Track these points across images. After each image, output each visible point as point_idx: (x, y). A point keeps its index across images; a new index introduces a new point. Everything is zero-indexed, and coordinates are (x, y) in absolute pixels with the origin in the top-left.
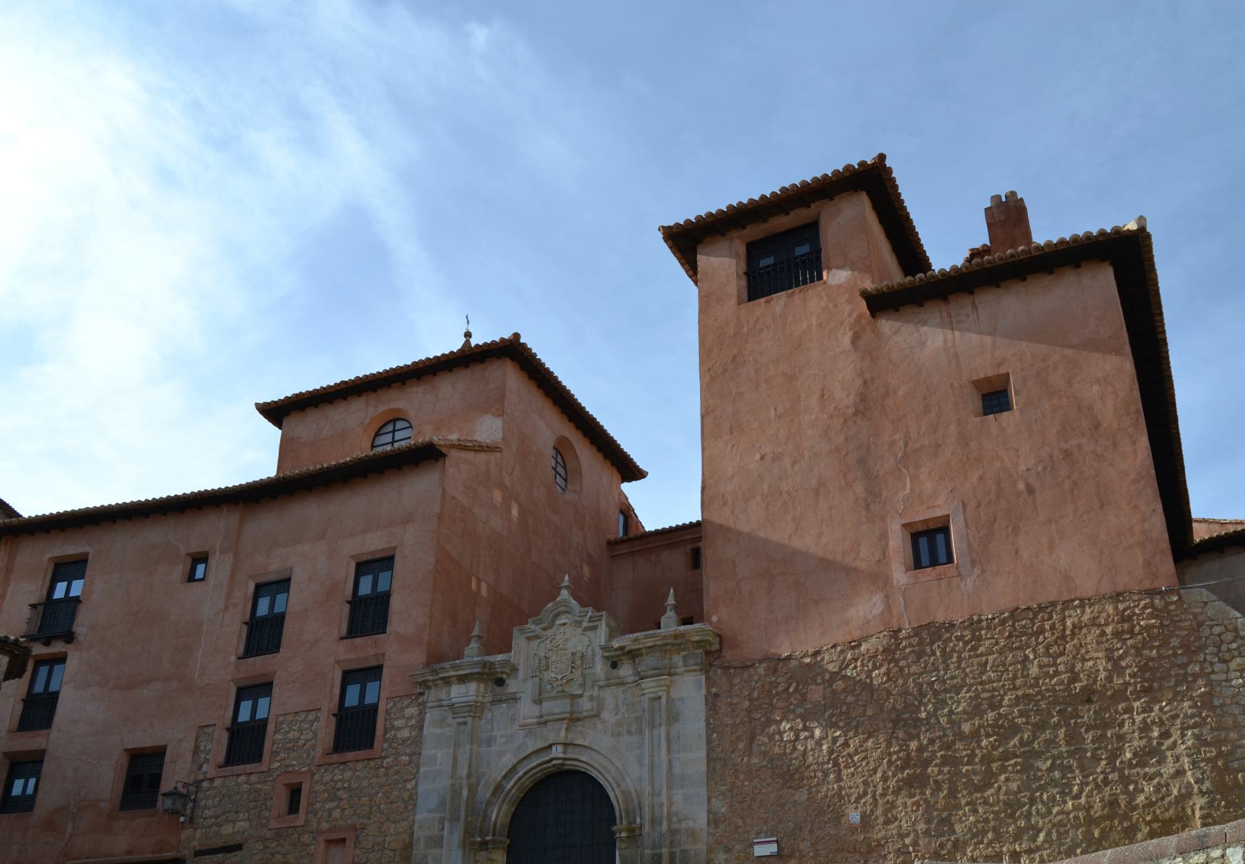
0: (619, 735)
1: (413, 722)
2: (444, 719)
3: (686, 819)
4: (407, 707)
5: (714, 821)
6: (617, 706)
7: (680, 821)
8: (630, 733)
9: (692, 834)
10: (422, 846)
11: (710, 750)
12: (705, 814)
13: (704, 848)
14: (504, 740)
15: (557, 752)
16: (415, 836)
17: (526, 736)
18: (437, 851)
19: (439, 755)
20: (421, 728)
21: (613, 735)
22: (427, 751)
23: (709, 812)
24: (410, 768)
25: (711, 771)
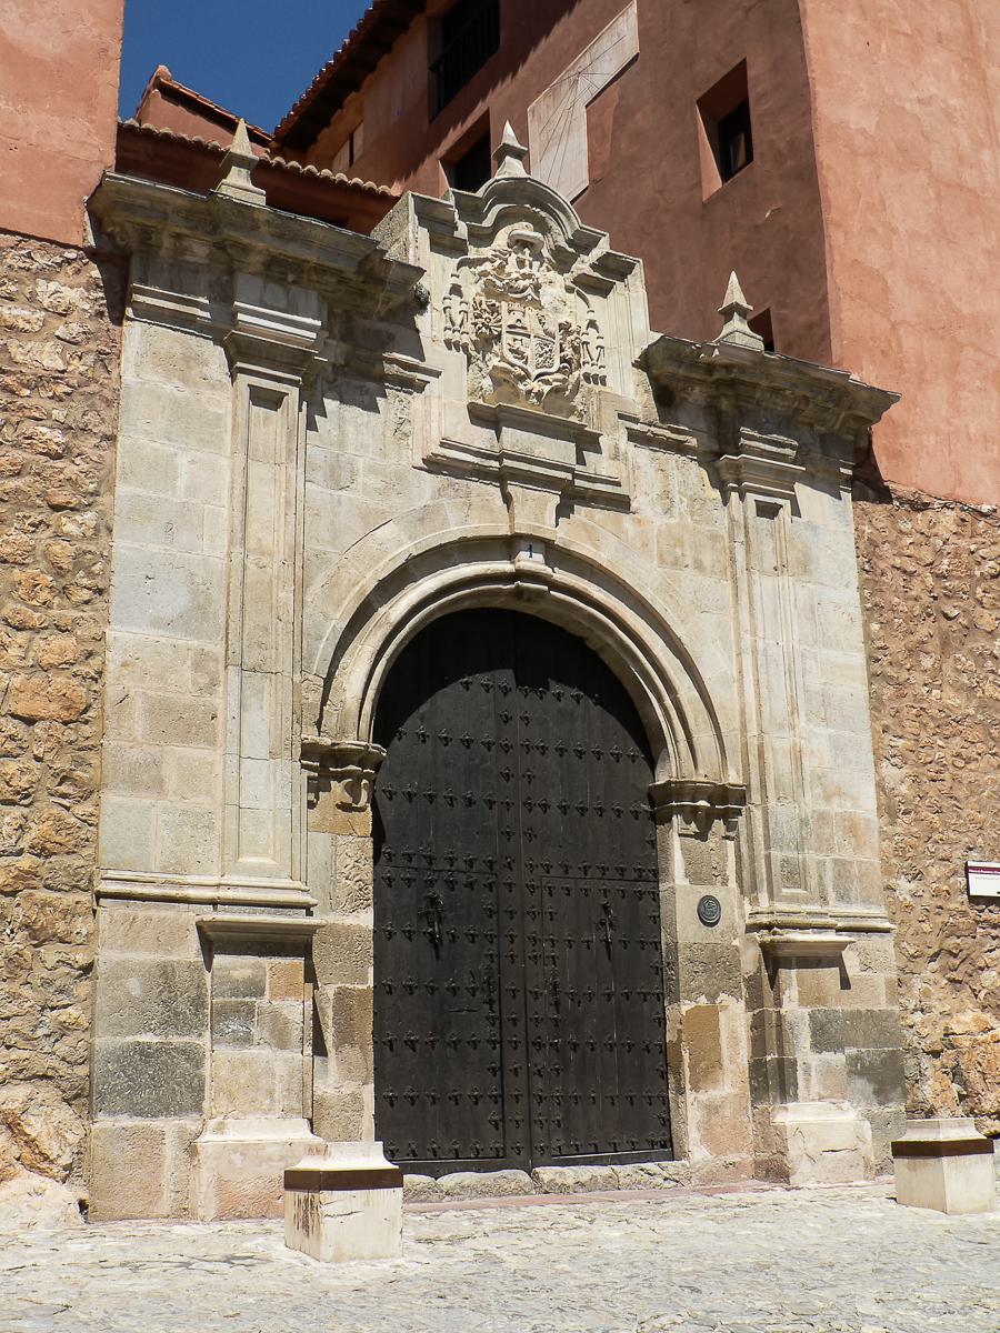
0: (675, 563)
1: (74, 328)
2: (191, 359)
3: (840, 793)
4: (47, 274)
5: (890, 809)
6: (666, 495)
7: (828, 798)
8: (699, 566)
9: (852, 828)
10: (138, 723)
11: (872, 659)
12: (872, 790)
13: (877, 861)
14: (374, 481)
15: (531, 561)
16: (112, 691)
17: (440, 492)
18: (194, 752)
19: (183, 461)
20: (107, 358)
21: (662, 560)
22: (139, 436)
23: (880, 786)
24: (70, 469)
25: (876, 704)
